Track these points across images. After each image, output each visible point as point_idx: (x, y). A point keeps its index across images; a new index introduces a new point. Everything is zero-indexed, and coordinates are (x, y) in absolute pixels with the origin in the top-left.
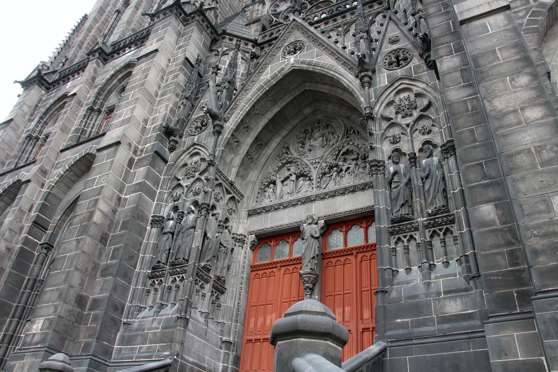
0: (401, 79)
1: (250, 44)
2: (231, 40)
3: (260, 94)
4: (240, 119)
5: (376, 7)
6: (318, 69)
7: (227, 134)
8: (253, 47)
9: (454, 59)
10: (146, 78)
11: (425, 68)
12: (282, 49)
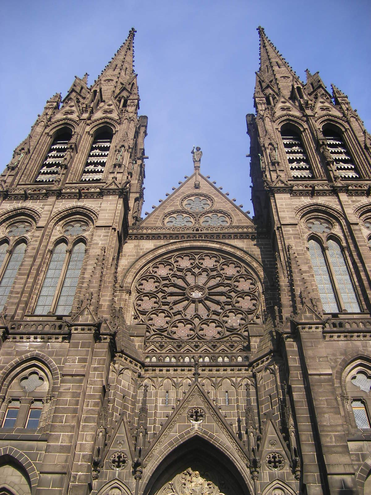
0: (277, 479)
1: (139, 365)
2: (126, 359)
3: (171, 449)
4: (155, 468)
5: (243, 371)
6: (217, 445)
7: (145, 479)
8: (140, 368)
9: (317, 488)
10: (77, 404)
11: (293, 477)
12: (187, 410)
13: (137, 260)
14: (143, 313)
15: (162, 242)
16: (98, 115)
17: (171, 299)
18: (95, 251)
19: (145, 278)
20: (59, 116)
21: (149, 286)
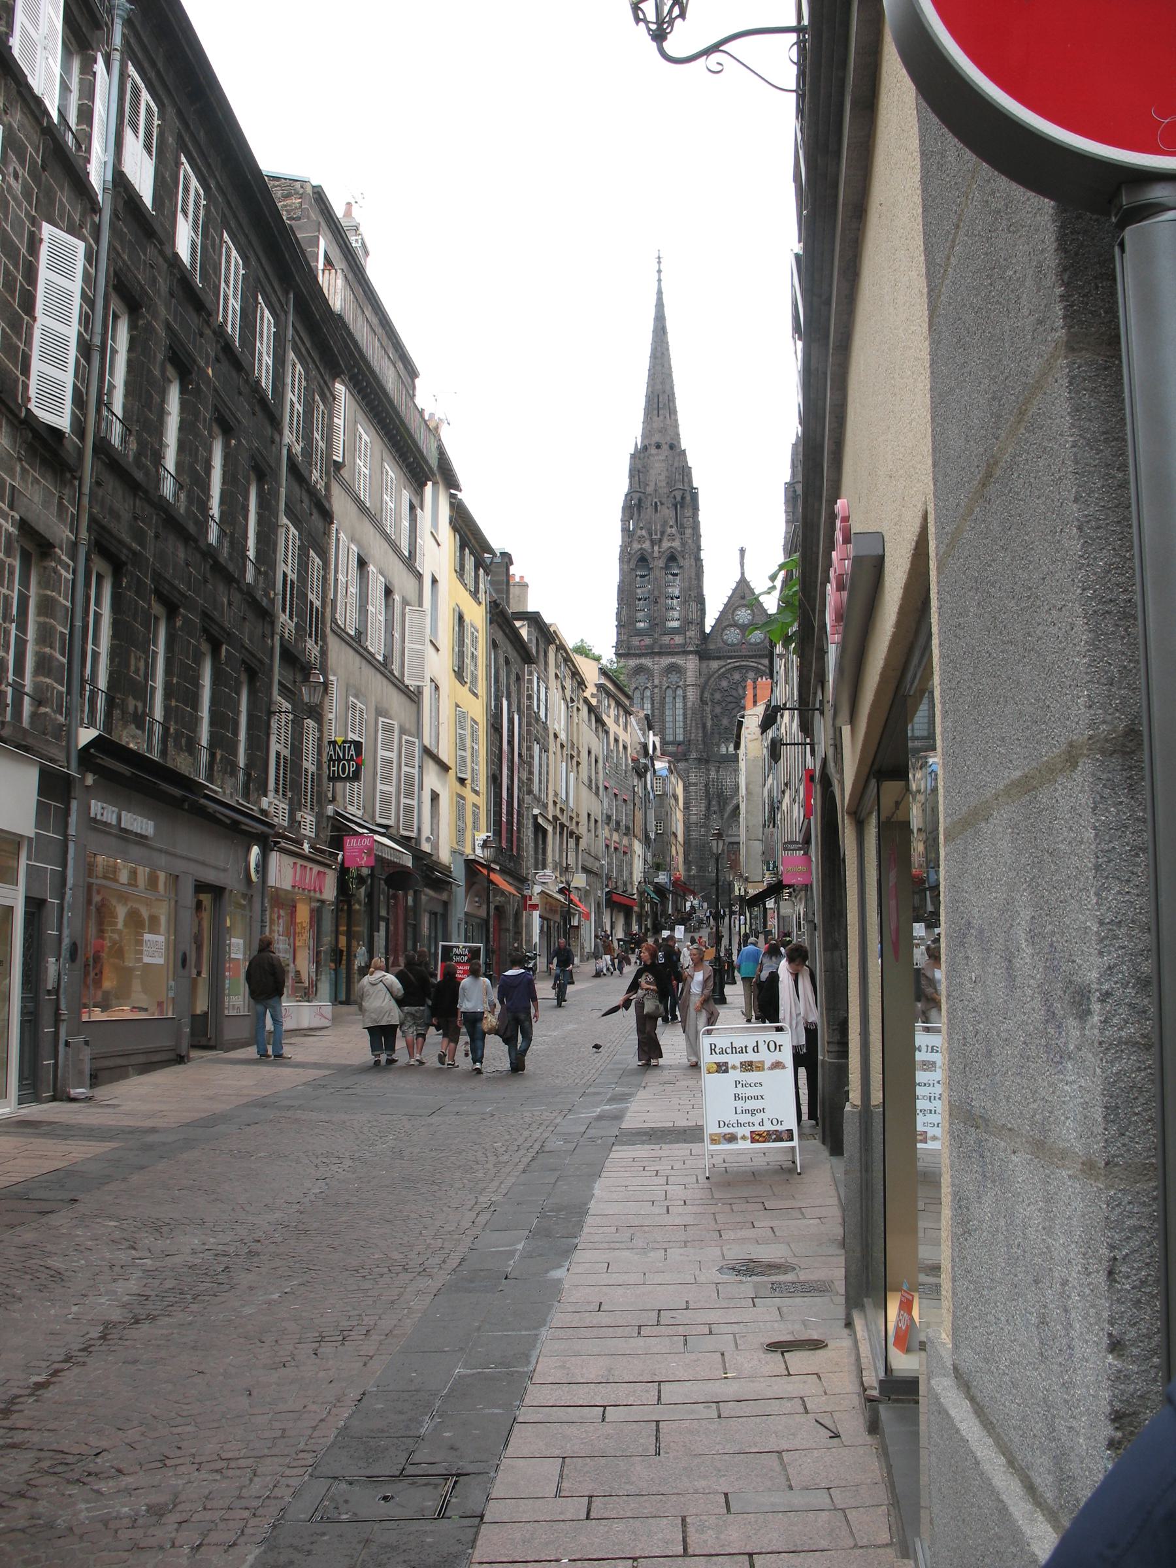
13: (709, 679)
14: (716, 717)
15: (722, 663)
16: (666, 544)
17: (731, 706)
18: (689, 705)
19: (715, 691)
20: (636, 546)
21: (718, 696)
